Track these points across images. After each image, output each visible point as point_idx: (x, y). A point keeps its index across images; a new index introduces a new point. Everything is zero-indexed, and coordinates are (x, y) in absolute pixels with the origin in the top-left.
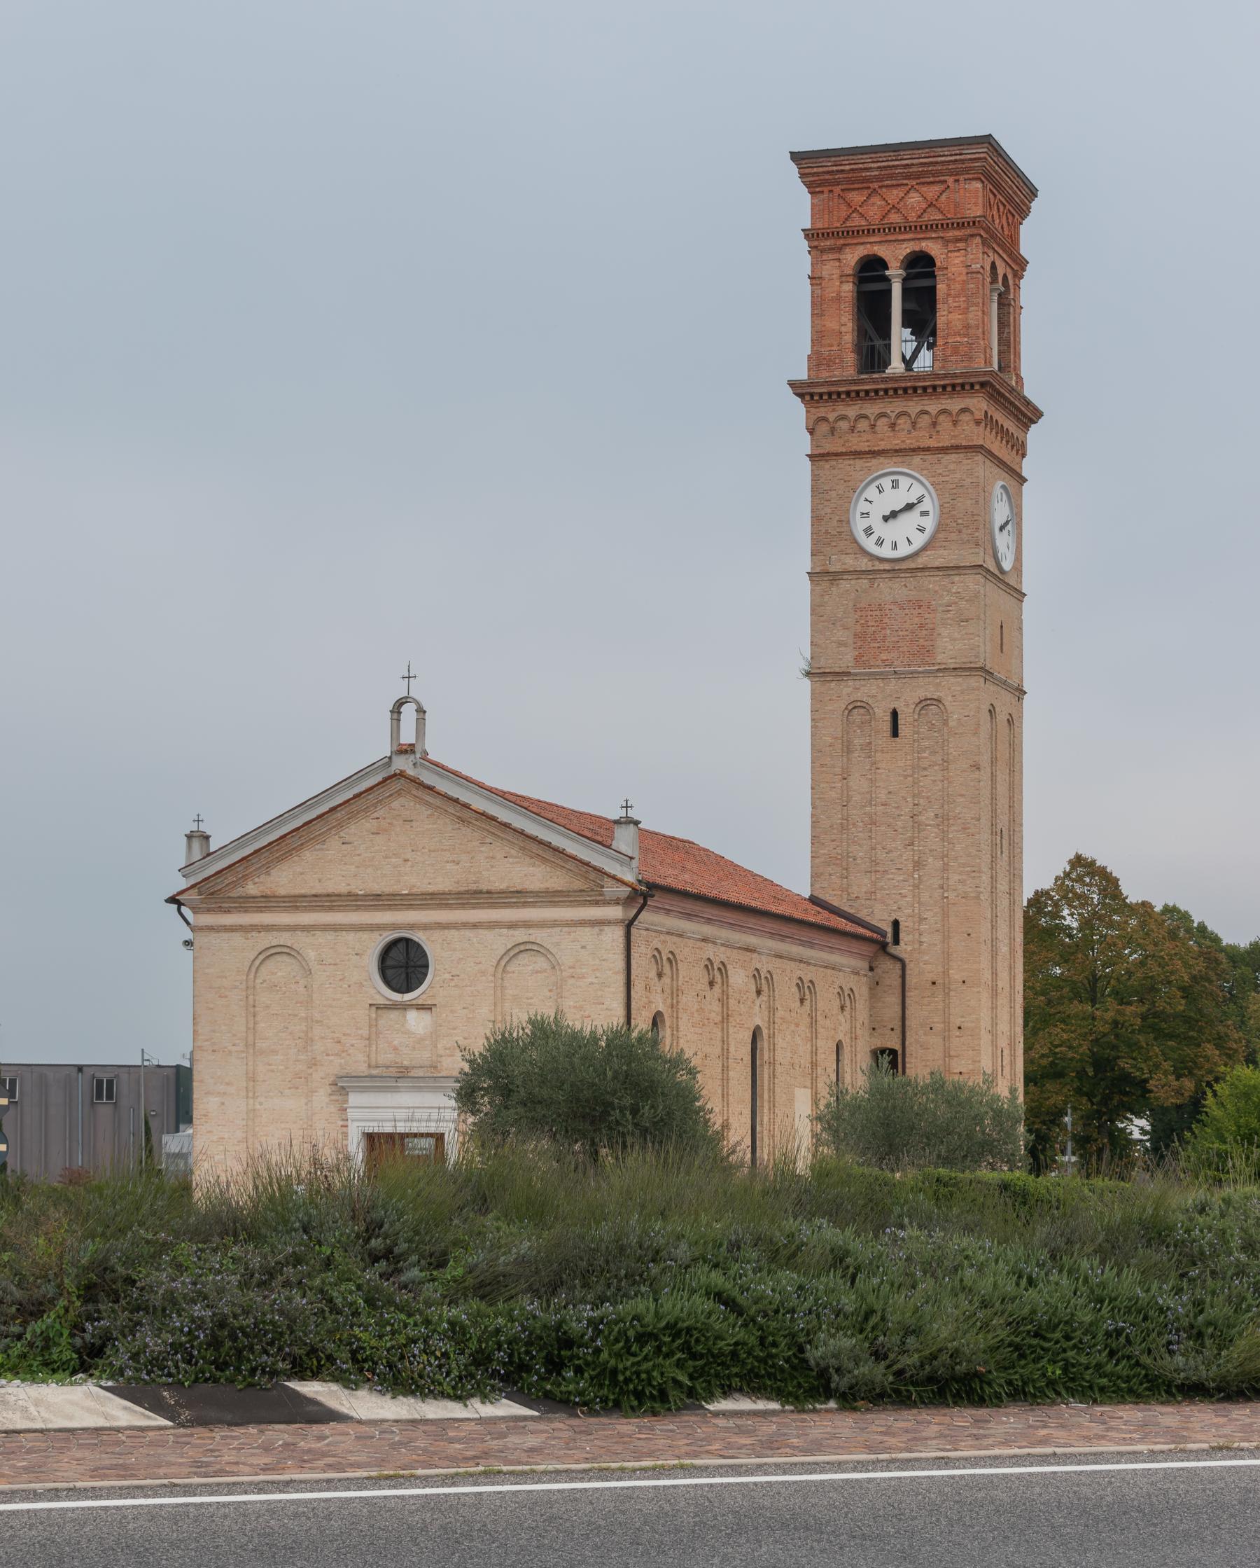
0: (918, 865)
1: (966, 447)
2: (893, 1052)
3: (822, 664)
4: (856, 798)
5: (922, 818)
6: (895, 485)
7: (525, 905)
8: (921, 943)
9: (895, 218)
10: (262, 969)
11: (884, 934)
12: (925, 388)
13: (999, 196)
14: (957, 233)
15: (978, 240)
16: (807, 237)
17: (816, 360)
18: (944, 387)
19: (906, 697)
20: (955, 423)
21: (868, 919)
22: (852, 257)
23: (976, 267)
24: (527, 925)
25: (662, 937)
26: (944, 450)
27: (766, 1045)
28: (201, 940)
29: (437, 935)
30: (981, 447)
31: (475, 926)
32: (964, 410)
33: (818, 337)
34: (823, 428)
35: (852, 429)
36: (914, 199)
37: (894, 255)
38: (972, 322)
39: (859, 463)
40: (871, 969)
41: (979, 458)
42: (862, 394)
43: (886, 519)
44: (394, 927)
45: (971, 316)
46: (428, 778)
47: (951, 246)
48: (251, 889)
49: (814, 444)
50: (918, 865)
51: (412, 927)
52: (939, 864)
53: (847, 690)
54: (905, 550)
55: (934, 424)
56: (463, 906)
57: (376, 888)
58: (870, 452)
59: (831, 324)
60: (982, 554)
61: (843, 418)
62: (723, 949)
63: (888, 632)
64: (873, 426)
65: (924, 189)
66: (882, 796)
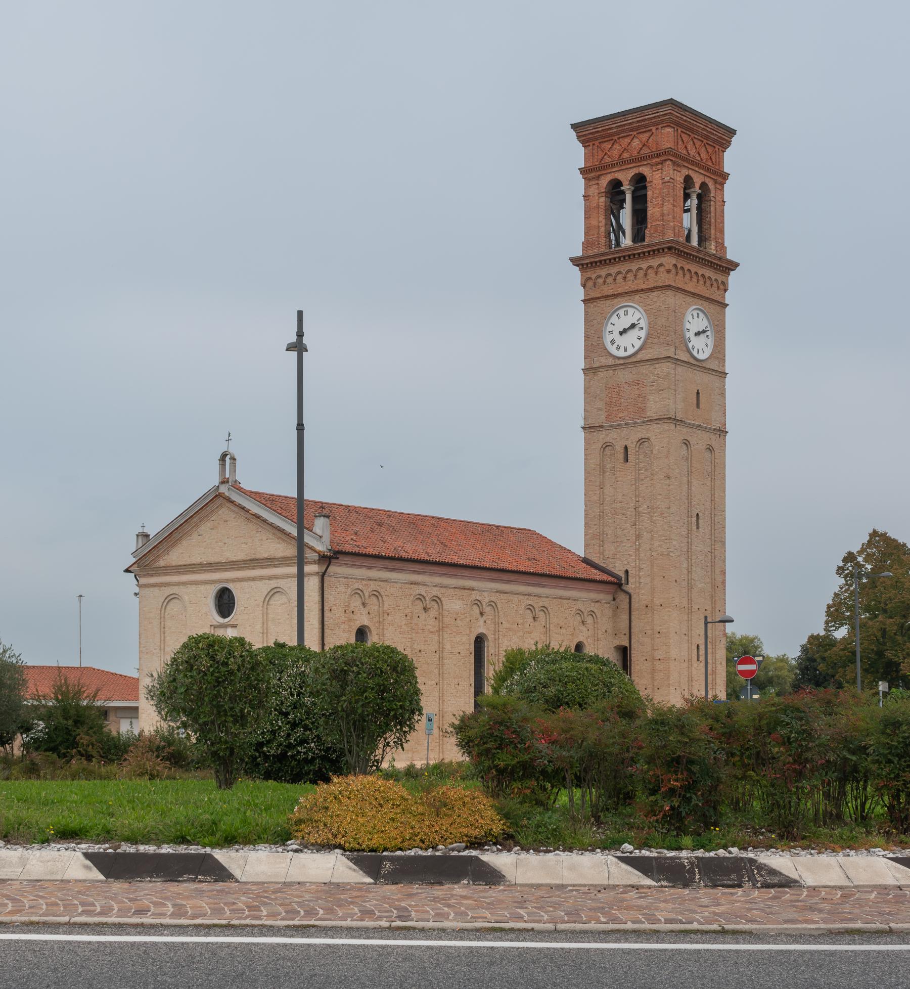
0: (638, 537)
1: (662, 287)
2: (626, 648)
3: (590, 422)
4: (608, 499)
5: (641, 509)
6: (626, 313)
7: (275, 566)
8: (640, 583)
9: (626, 155)
10: (168, 607)
11: (619, 578)
12: (639, 254)
13: (693, 135)
14: (657, 160)
15: (669, 162)
16: (581, 173)
17: (587, 245)
18: (649, 252)
19: (631, 437)
20: (656, 273)
21: (612, 570)
22: (604, 181)
23: (667, 179)
24: (275, 577)
25: (364, 582)
26: (650, 290)
27: (491, 644)
28: (147, 591)
29: (238, 585)
30: (669, 286)
31: (254, 579)
32: (661, 265)
33: (588, 230)
34: (590, 284)
35: (605, 281)
36: (636, 143)
37: (625, 177)
38: (665, 212)
39: (608, 302)
40: (614, 599)
41: (669, 293)
43: (621, 333)
44: (220, 581)
45: (665, 208)
46: (235, 497)
47: (654, 168)
48: (162, 563)
49: (586, 294)
50: (638, 537)
51: (227, 581)
52: (649, 536)
53: (602, 437)
54: (631, 351)
55: (646, 275)
56: (248, 568)
57: (212, 559)
58: (613, 295)
59: (594, 222)
60: (673, 350)
61: (599, 276)
62: (435, 589)
64: (615, 279)
65: (641, 136)
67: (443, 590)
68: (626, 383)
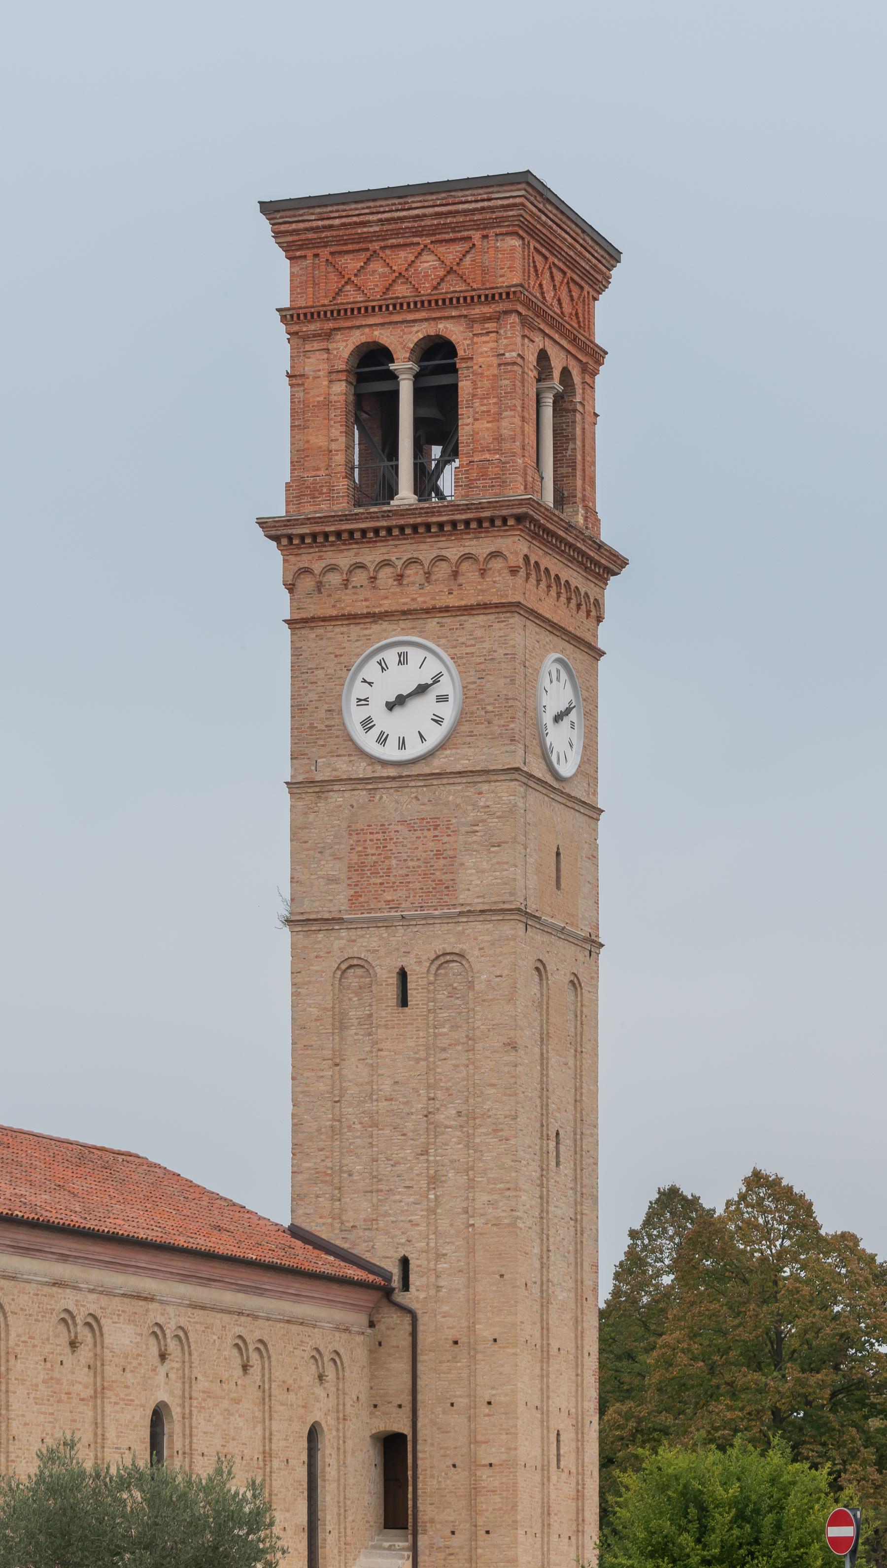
0: (434, 1181)
1: (497, 606)
3: (306, 907)
4: (352, 1090)
5: (440, 1117)
6: (403, 660)
8: (438, 1288)
9: (402, 290)
11: (386, 1276)
12: (441, 525)
13: (552, 259)
14: (487, 310)
15: (514, 318)
16: (283, 319)
17: (297, 490)
18: (467, 523)
19: (418, 950)
20: (483, 572)
21: (367, 1256)
22: (345, 346)
23: (510, 356)
27: (177, 1428)
30: (518, 604)
33: (300, 458)
34: (307, 583)
35: (346, 583)
36: (428, 264)
37: (402, 341)
38: (506, 433)
39: (355, 631)
40: (372, 1325)
41: (516, 620)
42: (357, 535)
43: (390, 706)
45: (504, 423)
47: (477, 329)
49: (295, 605)
50: (434, 1181)
53: (339, 944)
54: (415, 749)
55: (455, 574)
58: (368, 615)
59: (318, 440)
60: (521, 753)
61: (333, 568)
62: (93, 1296)
63: (394, 862)
64: (373, 579)
65: (442, 249)
66: (387, 1087)
67: (104, 1301)
68: (402, 822)
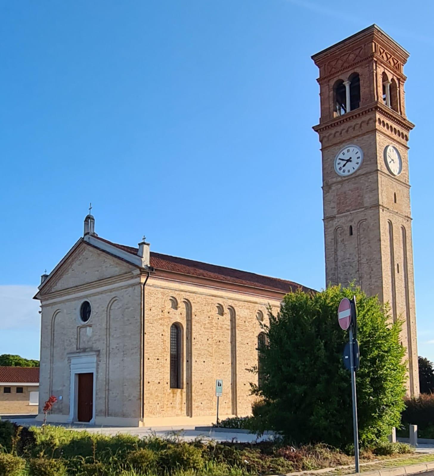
3: (327, 215)
4: (340, 258)
16: (318, 82)
36: (352, 56)
42: (336, 124)
51: (86, 296)
55: (361, 126)
63: (348, 200)
65: (355, 52)
66: (348, 256)
68: (349, 190)
